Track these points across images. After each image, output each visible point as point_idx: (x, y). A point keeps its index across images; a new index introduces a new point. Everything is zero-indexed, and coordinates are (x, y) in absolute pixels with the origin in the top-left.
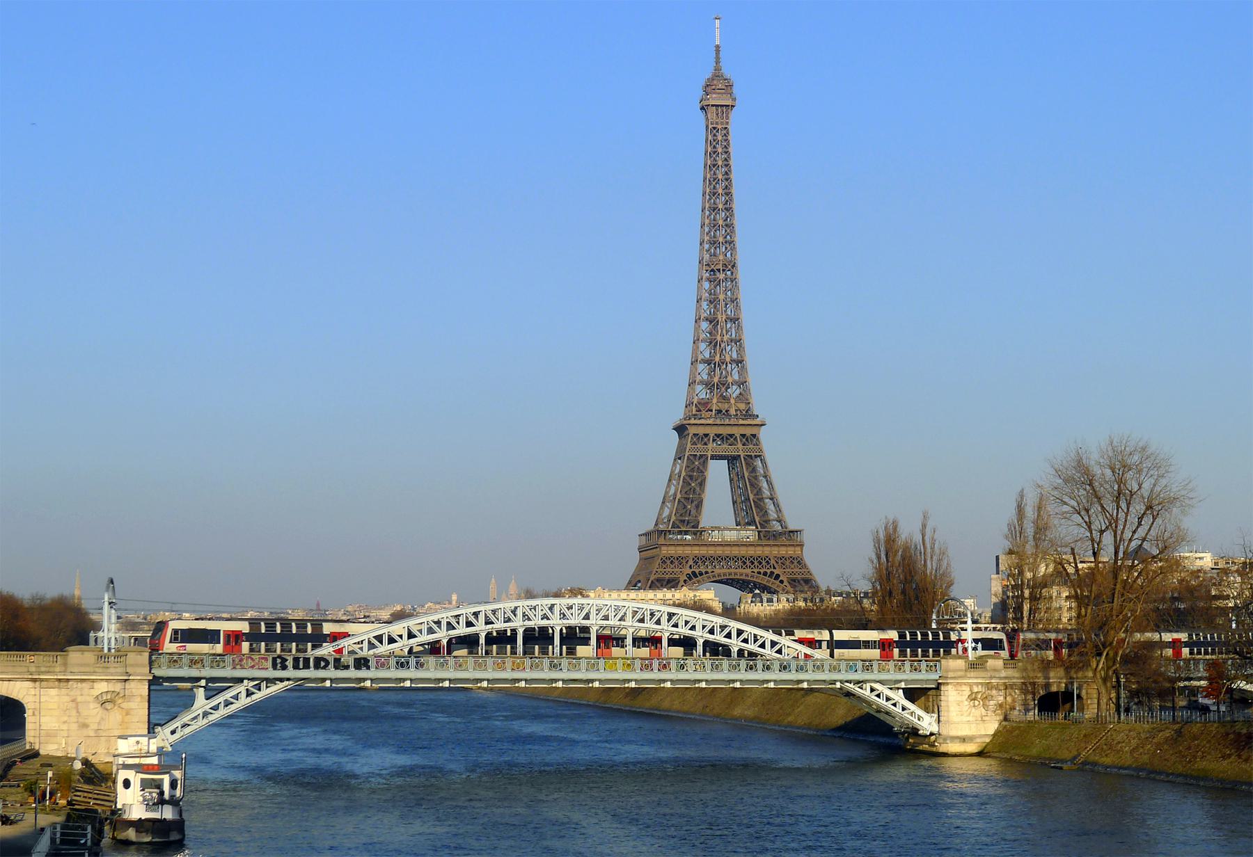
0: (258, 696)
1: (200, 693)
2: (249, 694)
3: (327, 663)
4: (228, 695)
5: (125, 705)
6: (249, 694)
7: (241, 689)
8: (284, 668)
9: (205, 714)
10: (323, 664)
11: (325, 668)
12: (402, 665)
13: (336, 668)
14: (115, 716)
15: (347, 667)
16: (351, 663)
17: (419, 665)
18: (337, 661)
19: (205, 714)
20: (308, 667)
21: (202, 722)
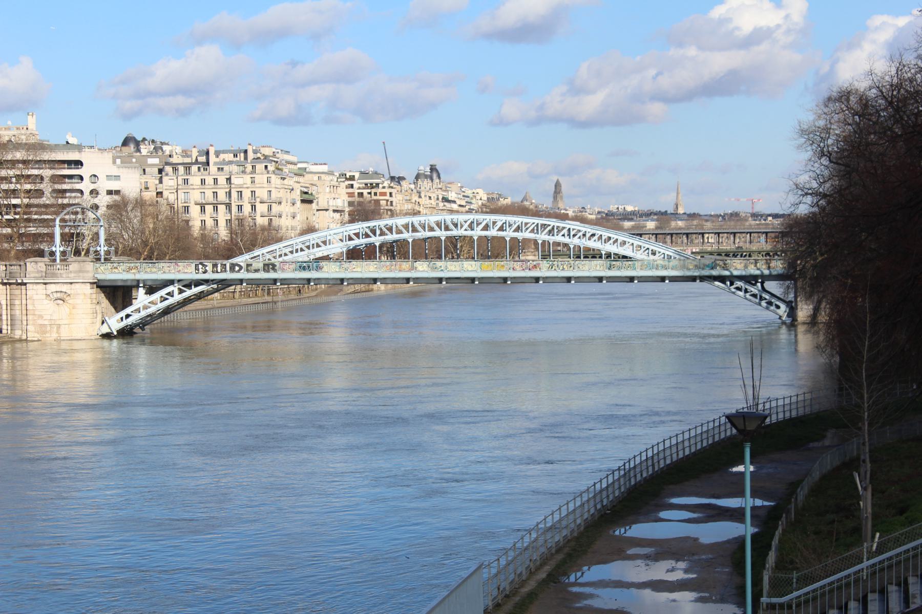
0: (188, 293)
1: (142, 291)
2: (181, 291)
3: (241, 268)
4: (163, 292)
5: (70, 301)
6: (181, 291)
7: (174, 288)
8: (205, 272)
9: (145, 308)
10: (237, 268)
11: (239, 271)
12: (304, 269)
13: (248, 271)
14: (64, 309)
15: (257, 271)
16: (261, 265)
17: (319, 268)
18: (248, 265)
19: (145, 308)
20: (226, 271)
21: (143, 313)
